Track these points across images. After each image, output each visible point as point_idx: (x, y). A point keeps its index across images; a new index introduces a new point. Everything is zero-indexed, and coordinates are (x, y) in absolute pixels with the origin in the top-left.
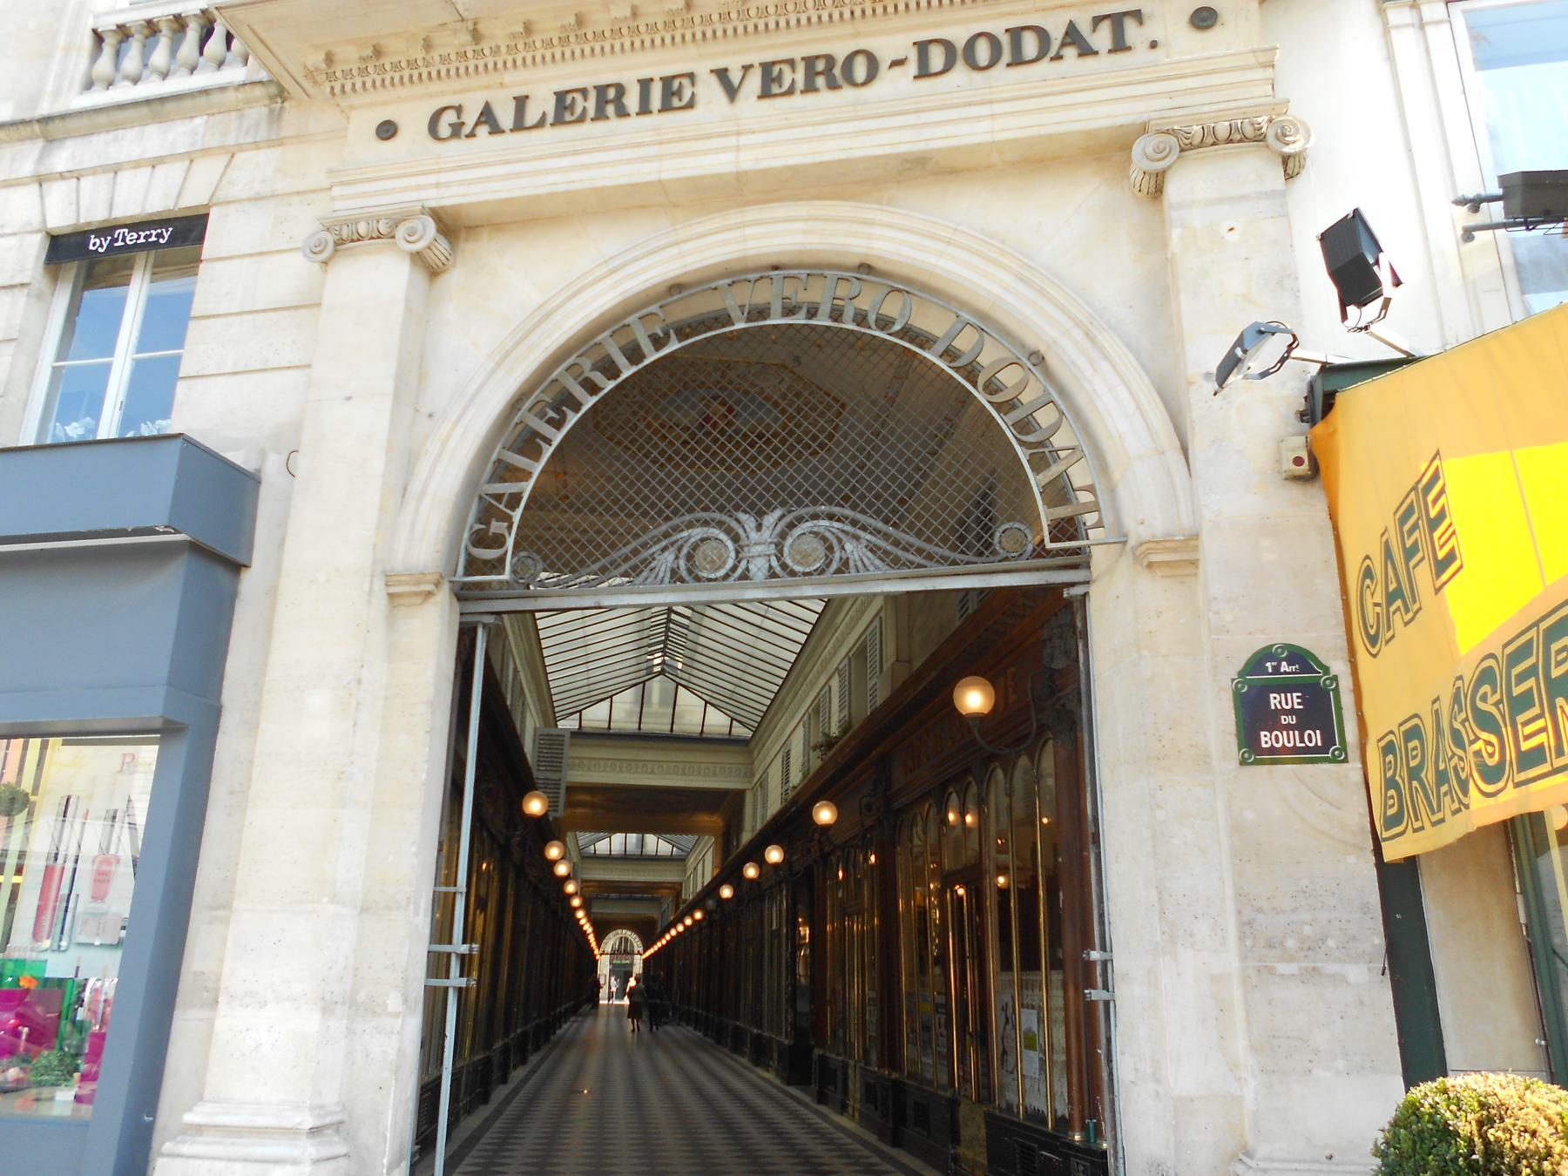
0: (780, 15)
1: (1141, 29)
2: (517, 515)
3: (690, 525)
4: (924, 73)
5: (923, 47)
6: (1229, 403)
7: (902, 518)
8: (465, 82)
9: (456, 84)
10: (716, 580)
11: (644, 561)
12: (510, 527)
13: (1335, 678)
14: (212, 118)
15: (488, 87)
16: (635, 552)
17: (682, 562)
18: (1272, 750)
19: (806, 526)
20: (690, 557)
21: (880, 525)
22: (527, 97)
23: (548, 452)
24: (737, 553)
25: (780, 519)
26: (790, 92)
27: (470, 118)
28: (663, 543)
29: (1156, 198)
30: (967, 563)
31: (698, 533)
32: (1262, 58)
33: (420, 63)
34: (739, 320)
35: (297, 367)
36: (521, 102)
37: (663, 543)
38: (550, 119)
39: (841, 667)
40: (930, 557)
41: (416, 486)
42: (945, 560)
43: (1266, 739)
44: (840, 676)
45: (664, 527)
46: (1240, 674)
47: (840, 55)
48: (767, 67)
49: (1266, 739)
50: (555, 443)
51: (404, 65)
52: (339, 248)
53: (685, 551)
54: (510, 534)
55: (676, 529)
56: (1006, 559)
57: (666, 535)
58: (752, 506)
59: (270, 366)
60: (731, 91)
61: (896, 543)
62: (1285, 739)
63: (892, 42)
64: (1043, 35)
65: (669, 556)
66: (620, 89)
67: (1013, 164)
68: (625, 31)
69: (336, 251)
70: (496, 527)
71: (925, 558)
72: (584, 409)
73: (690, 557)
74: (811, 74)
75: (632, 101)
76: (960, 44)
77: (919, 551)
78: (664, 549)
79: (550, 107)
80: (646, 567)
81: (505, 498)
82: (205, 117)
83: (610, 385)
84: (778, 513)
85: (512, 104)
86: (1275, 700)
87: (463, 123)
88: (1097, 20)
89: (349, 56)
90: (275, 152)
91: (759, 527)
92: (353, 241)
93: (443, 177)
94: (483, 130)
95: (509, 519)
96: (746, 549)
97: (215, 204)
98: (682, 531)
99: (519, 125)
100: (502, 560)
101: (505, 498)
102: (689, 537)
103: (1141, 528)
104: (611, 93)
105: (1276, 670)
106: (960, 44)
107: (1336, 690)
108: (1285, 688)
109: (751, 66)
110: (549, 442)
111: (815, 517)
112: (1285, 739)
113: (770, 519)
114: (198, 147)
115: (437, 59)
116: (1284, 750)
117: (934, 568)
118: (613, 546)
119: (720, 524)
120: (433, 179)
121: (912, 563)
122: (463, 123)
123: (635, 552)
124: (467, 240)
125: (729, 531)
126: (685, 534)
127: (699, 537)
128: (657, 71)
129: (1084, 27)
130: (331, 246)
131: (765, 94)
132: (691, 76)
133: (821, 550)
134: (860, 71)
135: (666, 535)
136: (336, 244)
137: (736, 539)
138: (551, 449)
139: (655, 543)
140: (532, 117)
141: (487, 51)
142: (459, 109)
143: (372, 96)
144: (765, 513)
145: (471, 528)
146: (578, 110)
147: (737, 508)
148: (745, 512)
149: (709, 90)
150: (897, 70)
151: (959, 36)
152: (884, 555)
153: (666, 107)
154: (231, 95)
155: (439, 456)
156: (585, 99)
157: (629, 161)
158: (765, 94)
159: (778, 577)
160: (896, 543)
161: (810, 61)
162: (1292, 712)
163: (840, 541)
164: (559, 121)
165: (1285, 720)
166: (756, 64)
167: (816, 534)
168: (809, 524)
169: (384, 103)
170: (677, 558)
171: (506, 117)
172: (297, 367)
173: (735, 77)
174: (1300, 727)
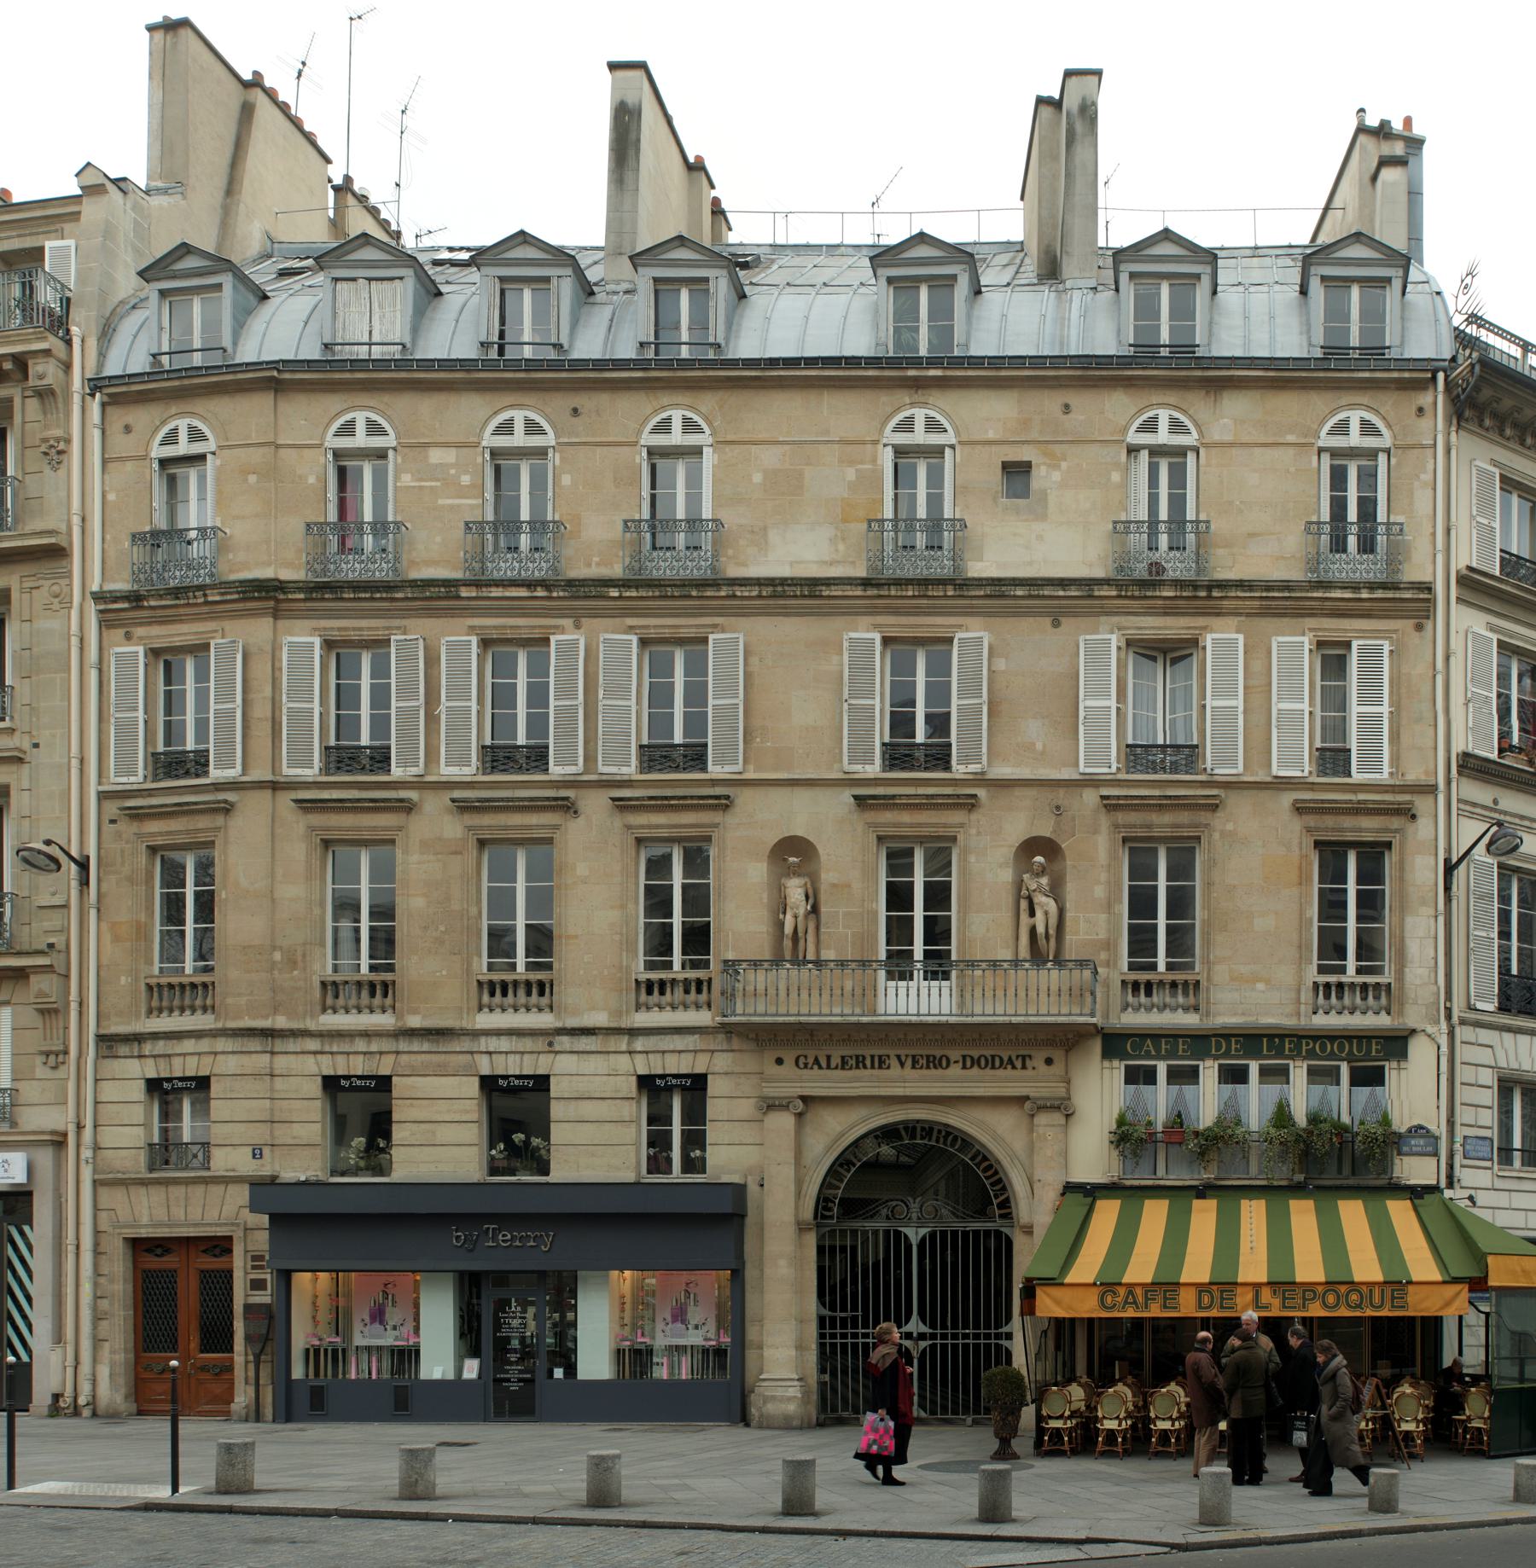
4: (964, 1067)
31: (894, 1203)
36: (829, 1058)
48: (914, 1057)
60: (902, 1065)
66: (864, 1058)
75: (868, 1063)
79: (839, 1061)
94: (816, 1067)
99: (828, 1067)
152: (954, 1214)
158: (913, 1067)
171: (824, 1063)
173: (903, 1059)
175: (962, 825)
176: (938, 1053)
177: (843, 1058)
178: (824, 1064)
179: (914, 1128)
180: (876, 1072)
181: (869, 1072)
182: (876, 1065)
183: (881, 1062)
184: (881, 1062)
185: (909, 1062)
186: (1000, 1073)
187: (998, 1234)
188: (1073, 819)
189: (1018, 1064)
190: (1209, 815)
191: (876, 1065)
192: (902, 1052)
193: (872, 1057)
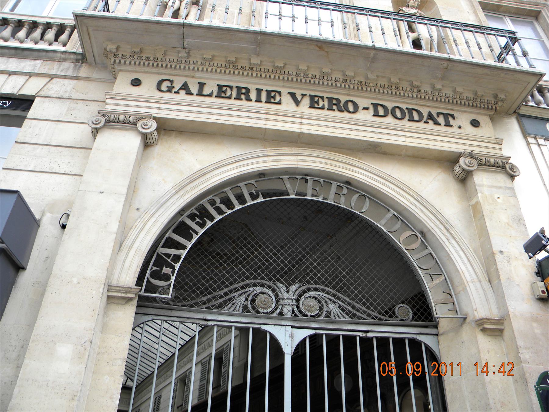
0: (320, 79)
2: (177, 266)
3: (255, 285)
4: (376, 115)
6: (510, 264)
7: (356, 296)
8: (177, 72)
9: (173, 72)
10: (267, 313)
11: (230, 299)
12: (173, 273)
14: (44, 62)
15: (186, 76)
16: (226, 294)
17: (249, 303)
19: (311, 293)
20: (253, 301)
22: (205, 84)
23: (195, 238)
24: (277, 302)
27: (177, 86)
28: (240, 292)
29: (462, 181)
30: (386, 320)
31: (258, 289)
33: (159, 60)
34: (292, 194)
35: (69, 174)
36: (202, 85)
37: (240, 292)
38: (215, 94)
39: (203, 361)
40: (369, 315)
41: (128, 242)
42: (374, 318)
44: (202, 365)
45: (241, 284)
48: (312, 97)
50: (200, 234)
51: (152, 59)
52: (106, 124)
53: (250, 298)
54: (173, 276)
55: (247, 286)
56: (402, 320)
57: (242, 288)
59: (54, 171)
60: (297, 103)
61: (353, 307)
64: (420, 113)
65: (243, 298)
66: (248, 90)
67: (409, 156)
68: (255, 69)
69: (104, 125)
70: (166, 270)
71: (367, 316)
72: (215, 221)
73: (253, 301)
75: (253, 96)
76: (390, 108)
77: (364, 312)
78: (241, 294)
80: (231, 302)
81: (172, 256)
82: (42, 61)
84: (297, 285)
85: (198, 86)
87: (174, 87)
89: (126, 50)
90: (74, 82)
91: (288, 292)
92: (115, 122)
93: (162, 106)
95: (173, 268)
96: (281, 301)
97: (38, 96)
98: (250, 287)
99: (200, 94)
101: (172, 256)
106: (390, 108)
109: (306, 95)
110: (197, 233)
111: (316, 290)
113: (293, 288)
114: (36, 72)
115: (168, 60)
118: (215, 290)
119: (269, 287)
122: (174, 87)
123: (226, 294)
124: (164, 135)
125: (274, 291)
126: (252, 289)
127: (259, 291)
128: (265, 88)
129: (435, 115)
130: (103, 122)
132: (280, 93)
133: (317, 306)
134: (351, 108)
135: (242, 288)
136: (106, 122)
137: (277, 295)
138: (198, 237)
139: (236, 291)
140: (206, 91)
141: (191, 62)
142: (172, 82)
143: (132, 68)
144: (292, 285)
145: (152, 268)
147: (278, 280)
148: (281, 283)
150: (365, 111)
151: (390, 105)
154: (59, 55)
157: (252, 118)
159: (298, 316)
160: (353, 307)
163: (326, 302)
166: (308, 95)
167: (316, 298)
168: (313, 292)
169: (136, 72)
170: (246, 300)
171: (194, 89)
172: (69, 174)
173: (299, 98)
177: (220, 87)
185: (306, 101)
187: (415, 344)
193: (259, 91)
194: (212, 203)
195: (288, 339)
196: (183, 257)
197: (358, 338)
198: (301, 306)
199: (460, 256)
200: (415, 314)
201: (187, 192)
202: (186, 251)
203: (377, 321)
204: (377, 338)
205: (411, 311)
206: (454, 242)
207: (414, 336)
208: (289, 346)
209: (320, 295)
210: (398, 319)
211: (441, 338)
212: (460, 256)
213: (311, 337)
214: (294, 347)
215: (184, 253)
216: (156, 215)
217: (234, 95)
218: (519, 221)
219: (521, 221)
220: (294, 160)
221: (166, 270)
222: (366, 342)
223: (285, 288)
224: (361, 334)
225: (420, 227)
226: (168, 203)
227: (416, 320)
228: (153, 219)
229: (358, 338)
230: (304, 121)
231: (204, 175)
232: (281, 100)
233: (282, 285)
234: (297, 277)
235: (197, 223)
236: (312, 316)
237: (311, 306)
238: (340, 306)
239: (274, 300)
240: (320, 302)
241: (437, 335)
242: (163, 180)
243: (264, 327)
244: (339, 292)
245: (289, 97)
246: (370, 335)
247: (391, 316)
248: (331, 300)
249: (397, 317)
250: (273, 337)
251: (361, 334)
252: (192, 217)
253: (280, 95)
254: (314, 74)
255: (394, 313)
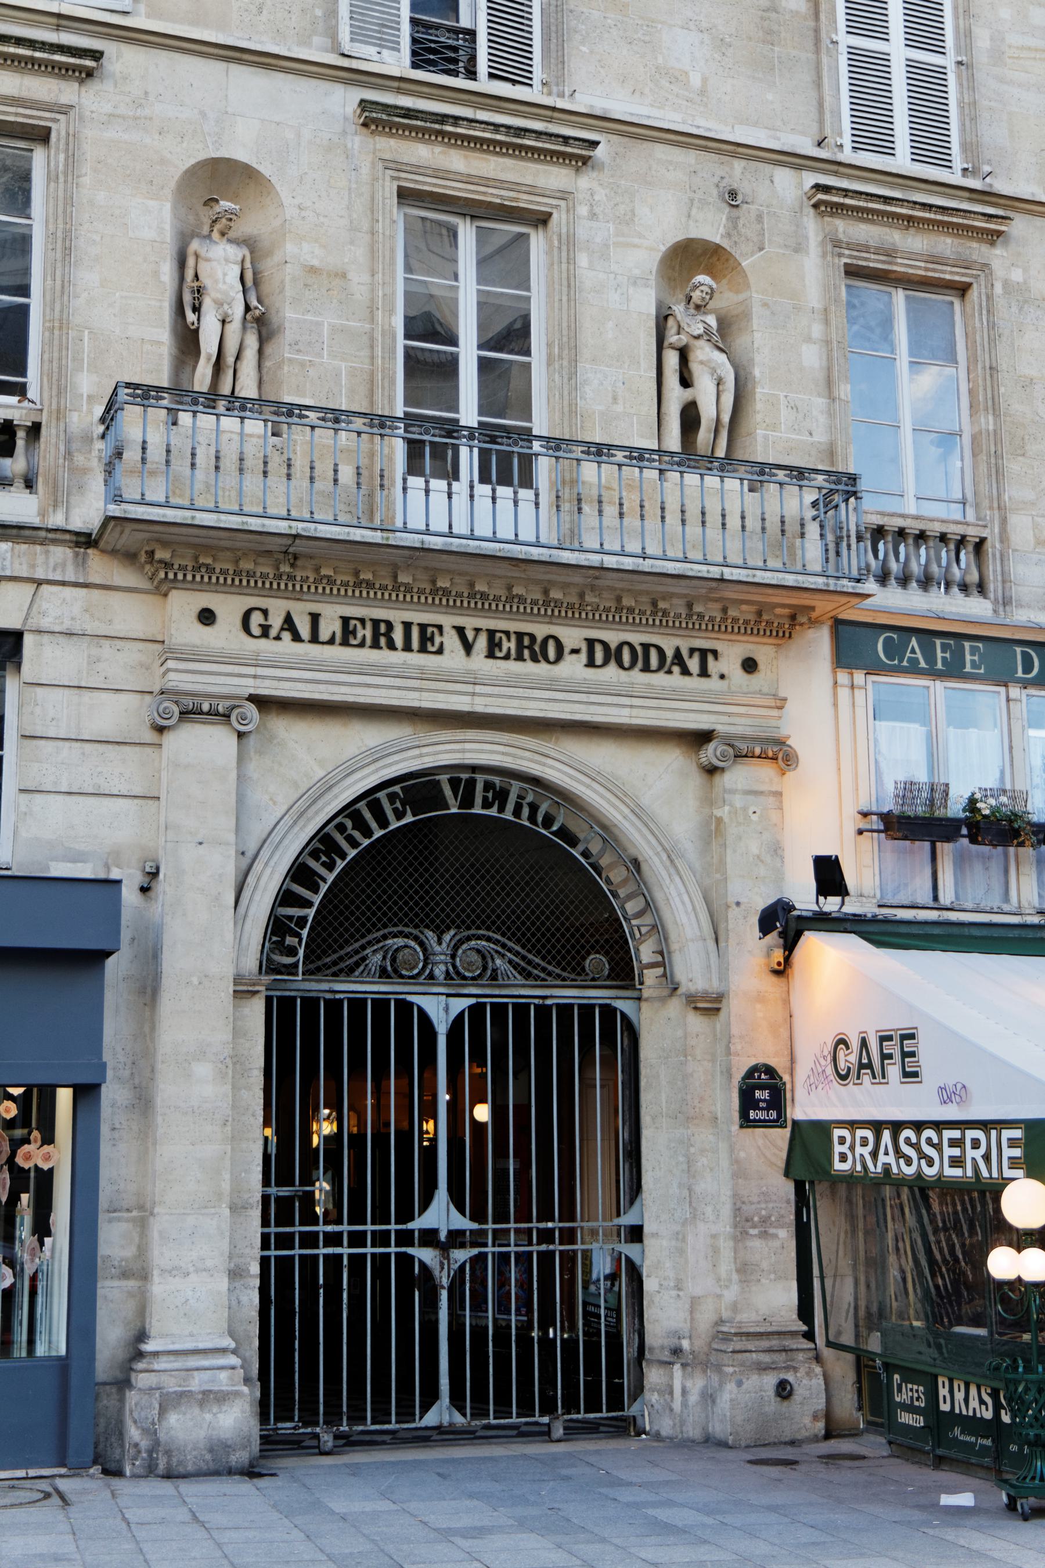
1: (716, 663)
3: (395, 936)
4: (591, 663)
5: (591, 643)
13: (784, 1084)
16: (357, 952)
18: (755, 1121)
20: (394, 960)
21: (499, 937)
23: (324, 888)
25: (454, 936)
26: (507, 657)
31: (400, 942)
32: (779, 703)
34: (454, 806)
36: (315, 618)
40: (549, 974)
43: (752, 1114)
46: (743, 1079)
47: (540, 635)
48: (491, 633)
49: (752, 1114)
50: (329, 882)
55: (385, 937)
56: (593, 979)
58: (438, 927)
60: (468, 647)
61: (529, 962)
62: (761, 1115)
63: (572, 636)
66: (390, 626)
72: (349, 858)
73: (394, 960)
74: (520, 647)
75: (398, 636)
76: (613, 646)
77: (544, 970)
79: (337, 627)
83: (366, 842)
84: (452, 932)
86: (758, 1094)
88: (692, 651)
91: (440, 943)
92: (194, 713)
93: (260, 671)
94: (286, 636)
96: (431, 957)
99: (315, 639)
100: (295, 965)
102: (394, 944)
103: (690, 984)
104: (383, 628)
105: (759, 1077)
106: (613, 646)
107: (785, 1090)
108: (762, 1087)
112: (761, 1115)
113: (447, 937)
116: (760, 1121)
117: (550, 981)
120: (251, 671)
121: (539, 977)
129: (685, 653)
131: (491, 655)
132: (440, 628)
138: (327, 887)
140: (324, 634)
142: (265, 612)
146: (359, 635)
147: (427, 927)
149: (451, 641)
150: (574, 656)
152: (522, 971)
153: (423, 649)
155: (255, 888)
156: (364, 628)
157: (399, 688)
158: (491, 655)
161: (520, 636)
162: (765, 1101)
164: (345, 643)
165: (762, 1105)
170: (384, 958)
171: (304, 629)
173: (470, 635)
174: (768, 1109)
175: (564, 195)
176: (541, 631)
177: (345, 620)
178: (305, 631)
179: (471, 783)
180: (416, 658)
181: (398, 657)
182: (415, 644)
183: (426, 640)
184: (426, 640)
185: (481, 644)
186: (659, 679)
187: (609, 1012)
188: (759, 218)
189: (693, 664)
190: (985, 248)
191: (415, 644)
192: (469, 623)
193: (407, 626)
194: (341, 828)
195: (442, 1014)
196: (310, 919)
197: (532, 1007)
198: (458, 963)
199: (683, 903)
200: (611, 969)
201: (309, 820)
202: (314, 909)
203: (559, 983)
204: (558, 1005)
205: (607, 966)
206: (677, 879)
207: (608, 1001)
208: (444, 1023)
209: (483, 946)
210: (590, 978)
211: (644, 1005)
212: (683, 903)
213: (470, 1007)
214: (450, 1022)
215: (311, 913)
216: (272, 863)
217: (368, 633)
218: (775, 851)
219: (779, 852)
220: (458, 751)
221: (290, 941)
222: (543, 1012)
223: (436, 939)
224: (536, 1001)
225: (633, 852)
226: (286, 842)
227: (613, 979)
228: (268, 871)
229: (532, 1007)
230: (478, 689)
231: (330, 788)
232: (442, 644)
233: (431, 933)
234: (453, 922)
235: (324, 864)
236: (473, 979)
237: (470, 963)
238: (510, 962)
239: (422, 957)
240: (484, 957)
241: (639, 999)
242: (271, 799)
243: (410, 998)
244: (510, 940)
245: (454, 632)
246: (549, 1002)
247: (579, 974)
248: (497, 952)
249: (587, 974)
250: (421, 1011)
251: (536, 1001)
252: (315, 854)
253: (441, 634)
254: (498, 593)
255: (583, 969)
